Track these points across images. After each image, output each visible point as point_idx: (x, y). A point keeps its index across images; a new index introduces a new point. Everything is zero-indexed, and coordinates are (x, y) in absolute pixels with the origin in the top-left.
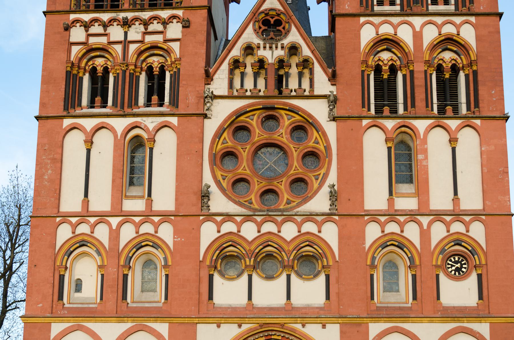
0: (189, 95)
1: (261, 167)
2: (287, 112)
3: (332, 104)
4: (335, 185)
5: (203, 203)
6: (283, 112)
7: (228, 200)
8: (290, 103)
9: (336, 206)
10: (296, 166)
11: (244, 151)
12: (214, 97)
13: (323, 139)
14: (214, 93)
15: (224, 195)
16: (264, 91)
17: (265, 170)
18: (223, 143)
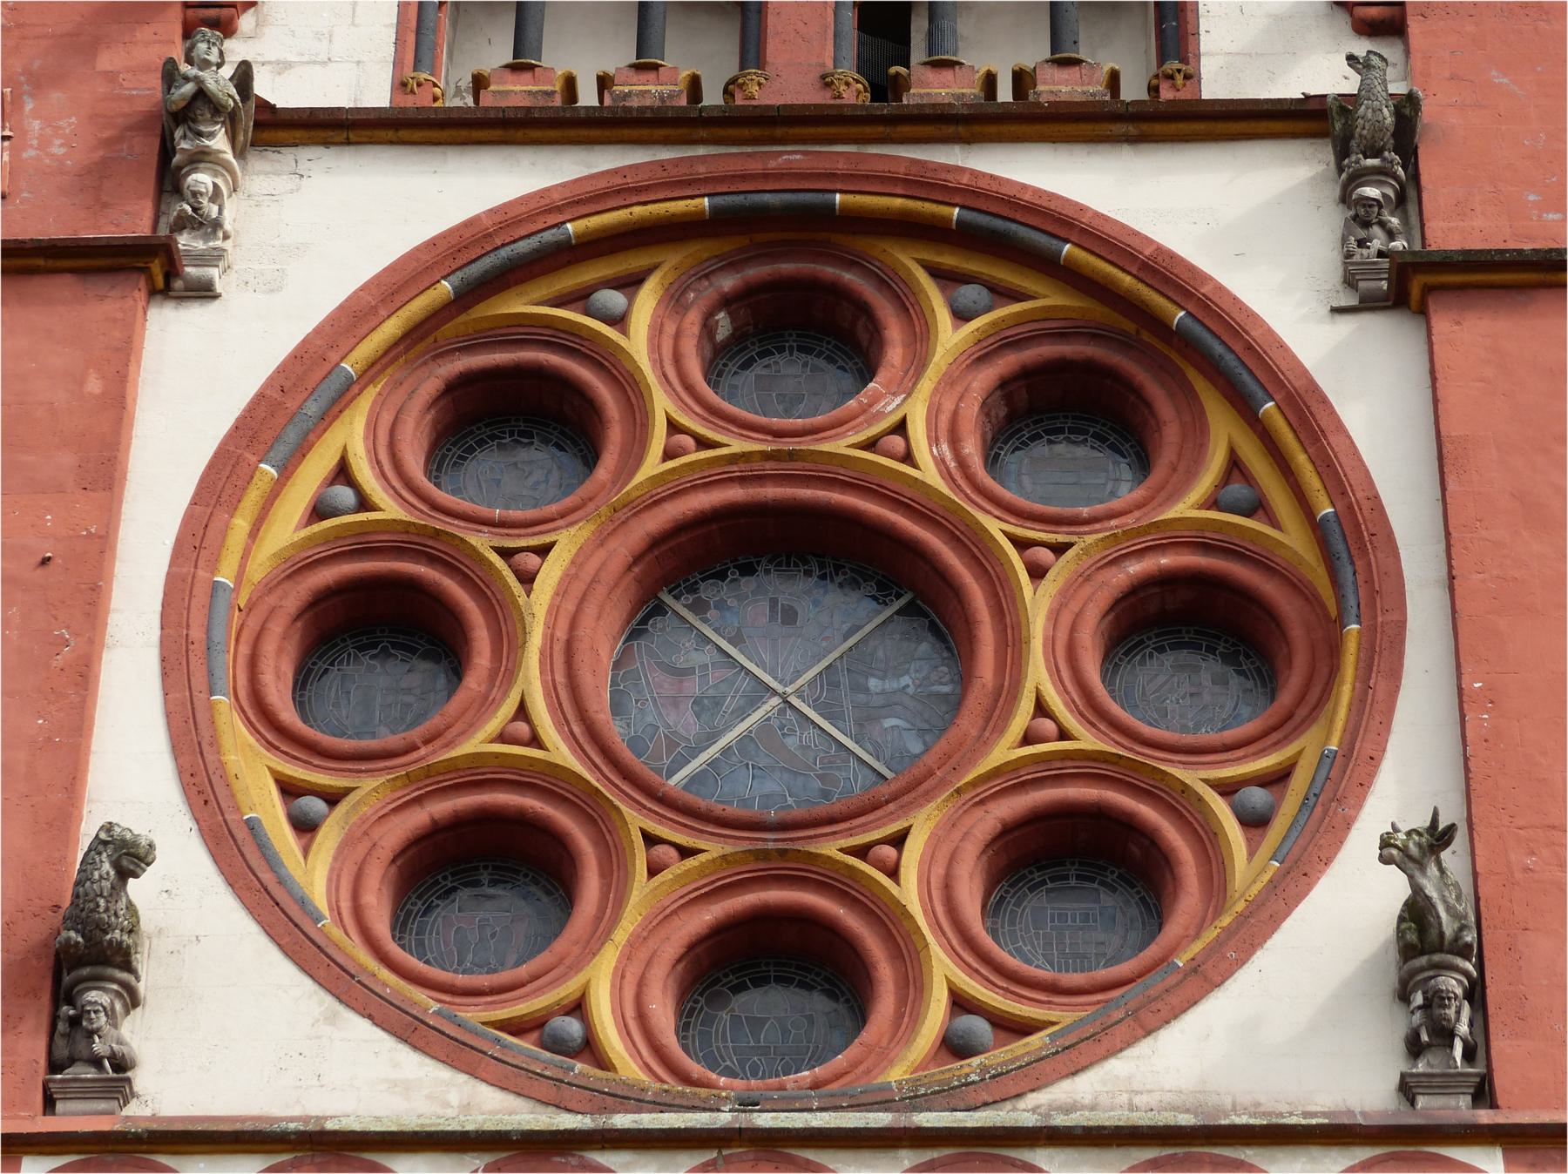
0: (29, 106)
1: (686, 723)
2: (949, 260)
3: (1370, 162)
4: (1451, 828)
5: (62, 1027)
6: (909, 261)
7: (329, 1000)
8: (975, 174)
9: (1469, 1055)
10: (1041, 709)
11: (527, 579)
12: (257, 125)
13: (1301, 460)
14: (263, 87)
15: (290, 953)
16: (733, 81)
17: (726, 751)
18: (319, 512)
